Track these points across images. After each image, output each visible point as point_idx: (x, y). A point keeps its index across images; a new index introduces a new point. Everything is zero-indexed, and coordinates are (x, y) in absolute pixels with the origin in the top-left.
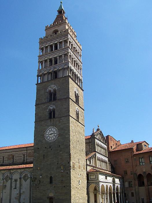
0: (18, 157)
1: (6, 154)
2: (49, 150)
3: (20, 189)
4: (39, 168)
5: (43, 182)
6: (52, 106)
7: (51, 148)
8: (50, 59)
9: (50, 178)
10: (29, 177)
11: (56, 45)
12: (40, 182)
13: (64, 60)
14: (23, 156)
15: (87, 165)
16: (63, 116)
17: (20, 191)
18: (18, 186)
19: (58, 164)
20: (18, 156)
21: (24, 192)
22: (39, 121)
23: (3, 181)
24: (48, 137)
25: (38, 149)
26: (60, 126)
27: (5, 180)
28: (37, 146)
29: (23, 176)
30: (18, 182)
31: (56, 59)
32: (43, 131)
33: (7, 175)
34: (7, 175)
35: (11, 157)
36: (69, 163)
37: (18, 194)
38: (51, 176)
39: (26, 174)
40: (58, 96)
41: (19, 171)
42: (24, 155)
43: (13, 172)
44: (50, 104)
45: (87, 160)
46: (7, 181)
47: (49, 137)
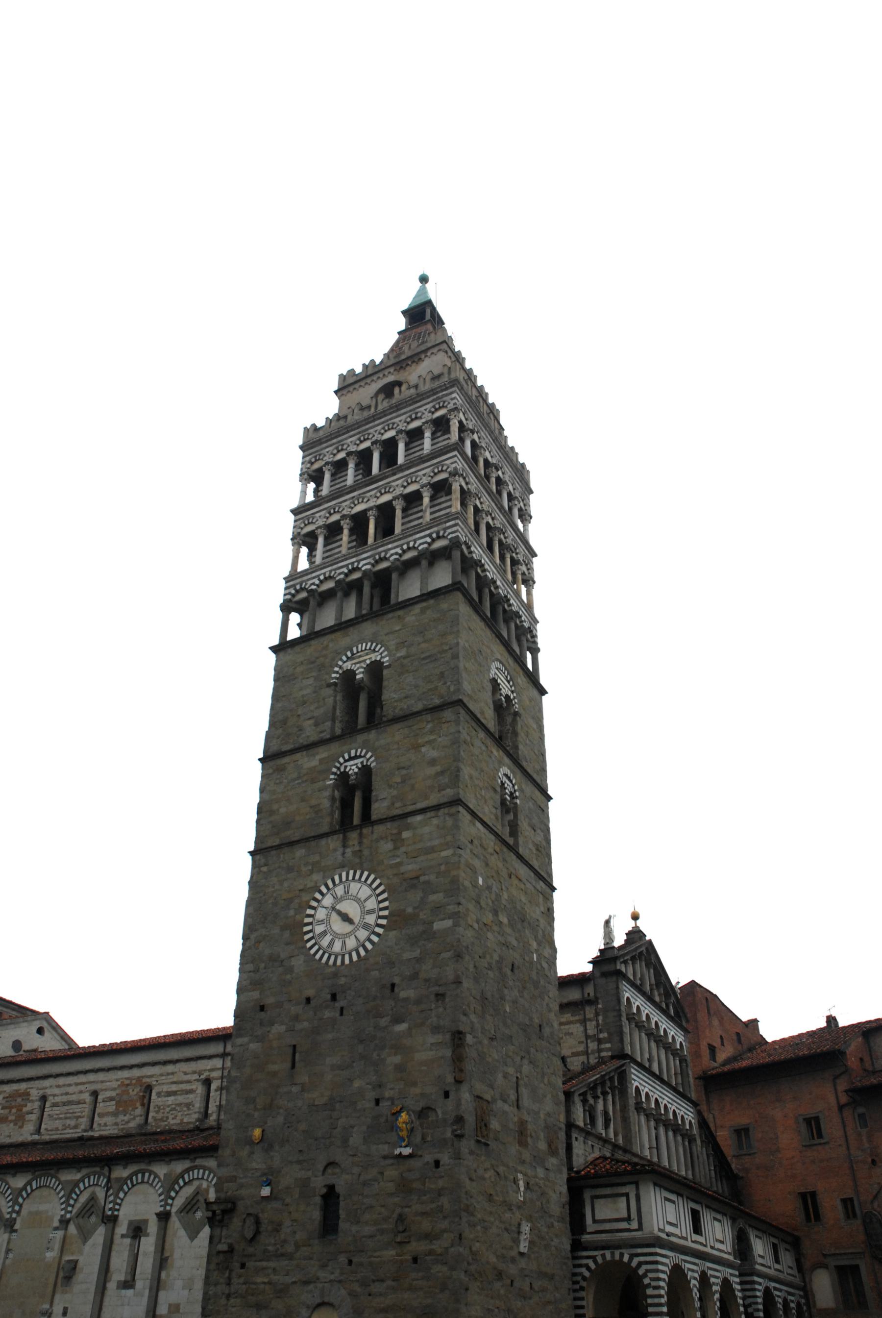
0: (174, 1093)
1: (112, 1075)
2: (327, 1014)
3: (157, 1285)
4: (257, 1132)
5: (277, 1228)
6: (356, 757)
7: (338, 1005)
9: (325, 1197)
11: (389, 449)
12: (257, 1233)
13: (431, 507)
14: (200, 1089)
15: (570, 1126)
16: (420, 806)
18: (146, 1265)
19: (377, 1102)
20: (174, 1088)
22: (277, 847)
23: (60, 1234)
24: (324, 933)
25: (262, 1008)
26: (400, 864)
27: (79, 1228)
28: (256, 995)
29: (179, 1202)
30: (148, 1244)
31: (386, 512)
32: (297, 901)
33: (93, 1198)
34: (93, 1198)
35: (135, 1092)
36: (452, 1095)
38: (331, 1188)
39: (197, 1193)
40: (393, 696)
41: (161, 1170)
42: (207, 1082)
43: (125, 1173)
44: (345, 748)
45: (568, 1095)
46: (85, 1235)
47: (328, 939)
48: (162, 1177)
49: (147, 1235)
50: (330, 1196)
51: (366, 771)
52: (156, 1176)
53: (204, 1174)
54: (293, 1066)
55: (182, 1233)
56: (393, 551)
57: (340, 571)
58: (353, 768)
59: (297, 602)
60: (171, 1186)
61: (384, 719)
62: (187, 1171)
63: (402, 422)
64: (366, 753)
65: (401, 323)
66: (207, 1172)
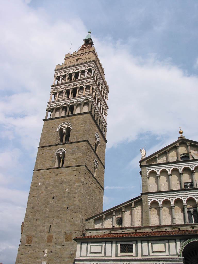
6: (62, 150)
8: (67, 90)
11: (77, 74)
51: (64, 154)
56: (75, 100)
57: (61, 103)
58: (61, 152)
59: (51, 109)
61: (69, 142)
63: (81, 69)
64: (65, 149)
65: (83, 43)
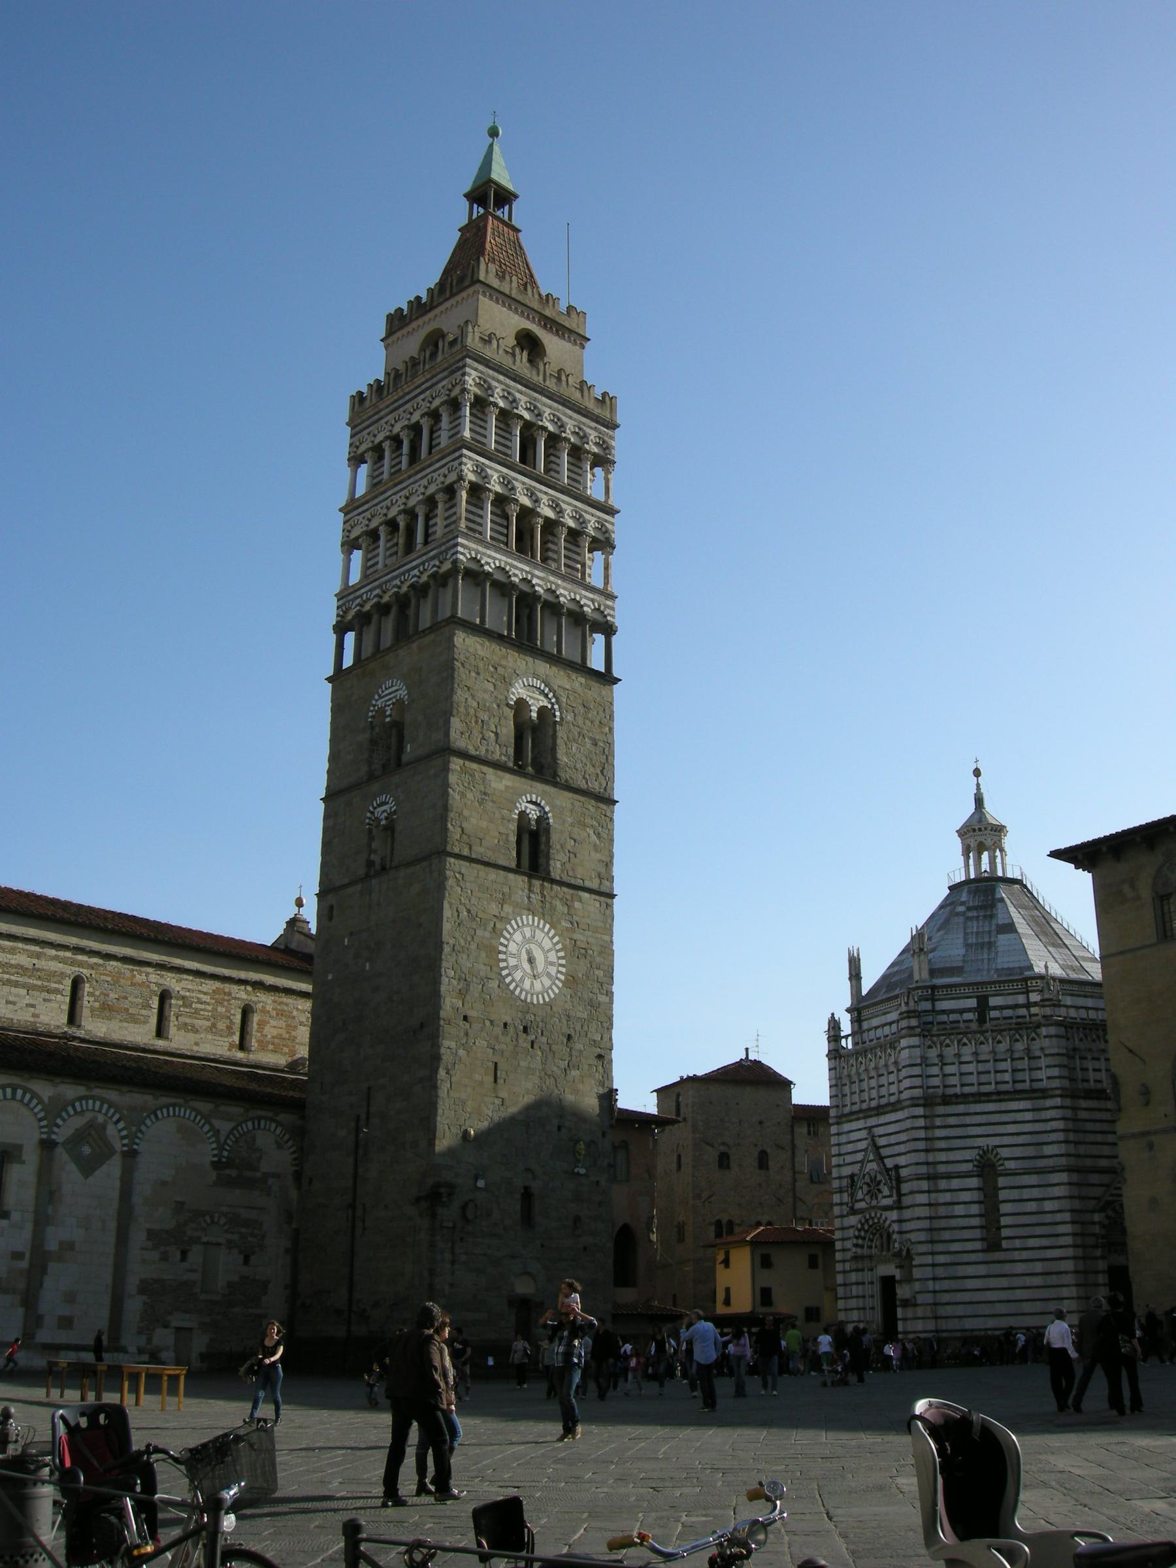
10: (118, 1145)
17: (37, 1244)
19: (559, 1128)
21: (68, 1246)
37: (17, 1256)
39: (91, 1125)
41: (45, 1089)
48: (46, 1100)
49: (23, 1163)
50: (527, 1195)
52: (34, 1095)
53: (101, 1107)
54: (495, 1081)
55: (72, 1167)
60: (55, 1111)
62: (80, 1099)
66: (106, 1106)
